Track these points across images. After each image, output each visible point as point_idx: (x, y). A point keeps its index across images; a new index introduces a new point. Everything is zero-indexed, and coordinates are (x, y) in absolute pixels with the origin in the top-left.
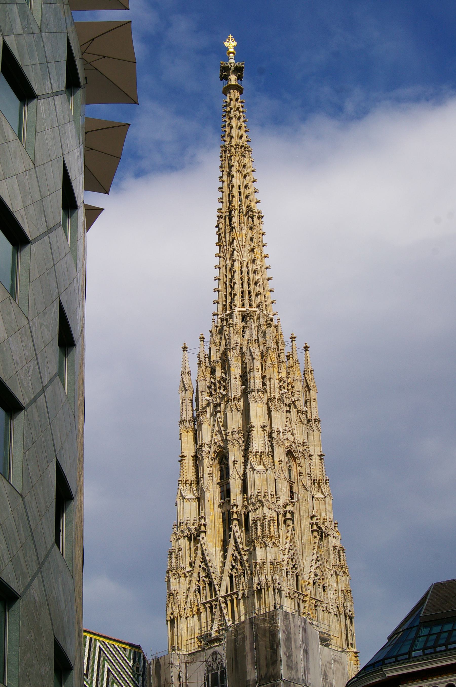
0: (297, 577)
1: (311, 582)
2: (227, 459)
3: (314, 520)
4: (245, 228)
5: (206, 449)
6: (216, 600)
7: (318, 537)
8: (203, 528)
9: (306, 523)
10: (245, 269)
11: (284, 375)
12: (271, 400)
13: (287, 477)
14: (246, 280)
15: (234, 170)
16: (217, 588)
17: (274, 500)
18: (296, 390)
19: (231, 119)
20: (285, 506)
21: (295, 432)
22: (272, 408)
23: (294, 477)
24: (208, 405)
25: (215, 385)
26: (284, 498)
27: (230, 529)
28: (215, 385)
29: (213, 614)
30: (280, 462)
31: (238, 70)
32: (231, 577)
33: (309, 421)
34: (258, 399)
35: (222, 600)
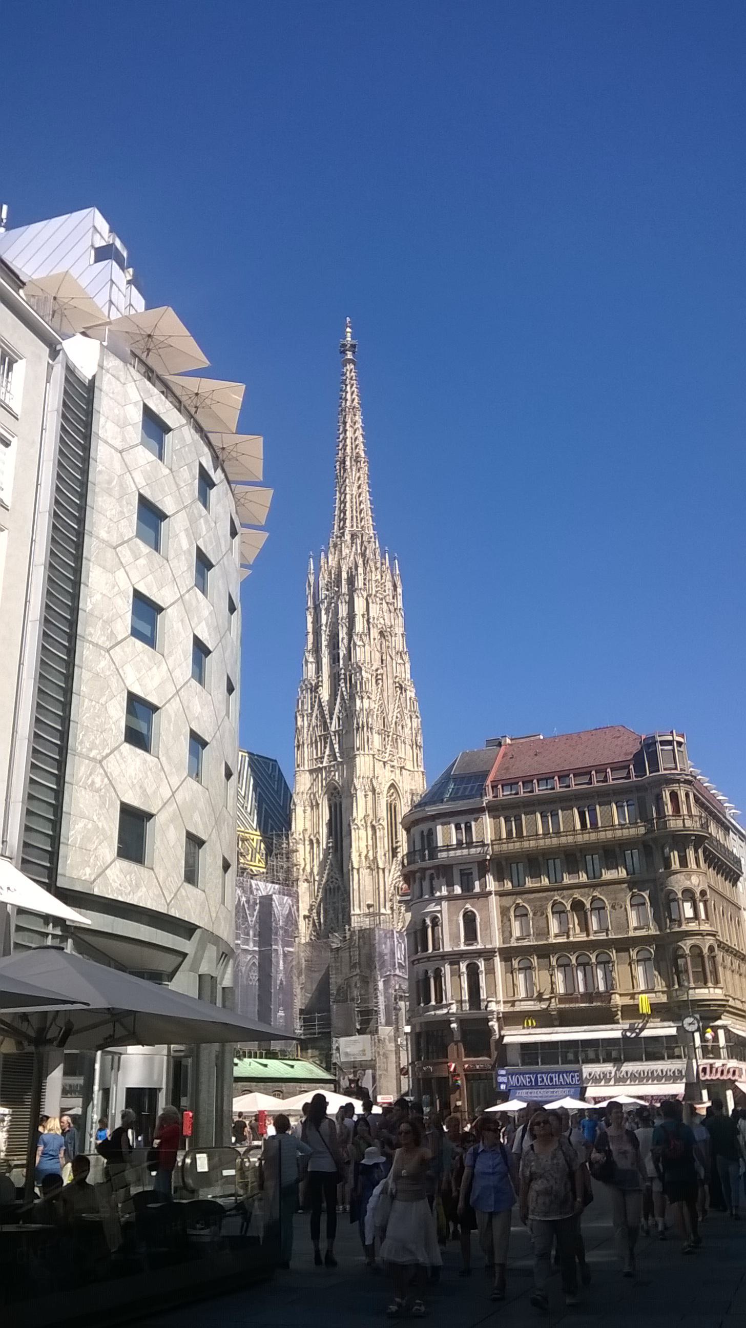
0: (384, 719)
1: (394, 722)
2: (338, 636)
3: (397, 680)
4: (354, 468)
5: (323, 628)
6: (329, 734)
7: (399, 692)
8: (320, 684)
9: (390, 681)
10: (354, 500)
11: (379, 577)
12: (369, 595)
13: (379, 649)
14: (354, 507)
15: (348, 425)
16: (329, 725)
17: (369, 666)
18: (387, 588)
19: (346, 385)
20: (377, 670)
21: (386, 618)
22: (370, 601)
23: (384, 650)
24: (326, 598)
25: (331, 583)
26: (377, 664)
27: (339, 685)
28: (331, 583)
29: (326, 743)
30: (374, 639)
31: (353, 346)
32: (339, 718)
33: (395, 609)
34: (360, 595)
35: (332, 734)
